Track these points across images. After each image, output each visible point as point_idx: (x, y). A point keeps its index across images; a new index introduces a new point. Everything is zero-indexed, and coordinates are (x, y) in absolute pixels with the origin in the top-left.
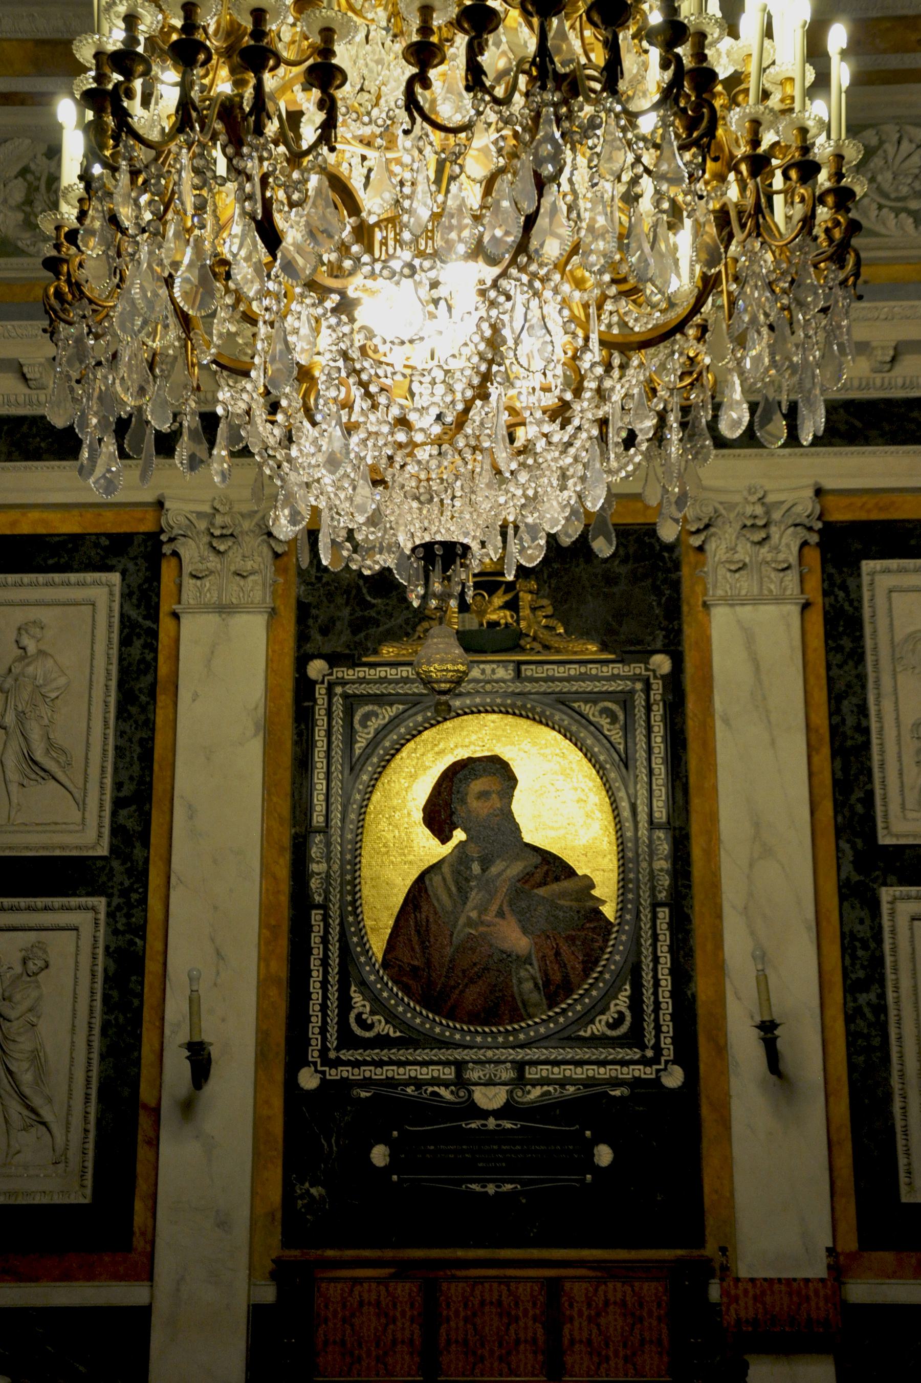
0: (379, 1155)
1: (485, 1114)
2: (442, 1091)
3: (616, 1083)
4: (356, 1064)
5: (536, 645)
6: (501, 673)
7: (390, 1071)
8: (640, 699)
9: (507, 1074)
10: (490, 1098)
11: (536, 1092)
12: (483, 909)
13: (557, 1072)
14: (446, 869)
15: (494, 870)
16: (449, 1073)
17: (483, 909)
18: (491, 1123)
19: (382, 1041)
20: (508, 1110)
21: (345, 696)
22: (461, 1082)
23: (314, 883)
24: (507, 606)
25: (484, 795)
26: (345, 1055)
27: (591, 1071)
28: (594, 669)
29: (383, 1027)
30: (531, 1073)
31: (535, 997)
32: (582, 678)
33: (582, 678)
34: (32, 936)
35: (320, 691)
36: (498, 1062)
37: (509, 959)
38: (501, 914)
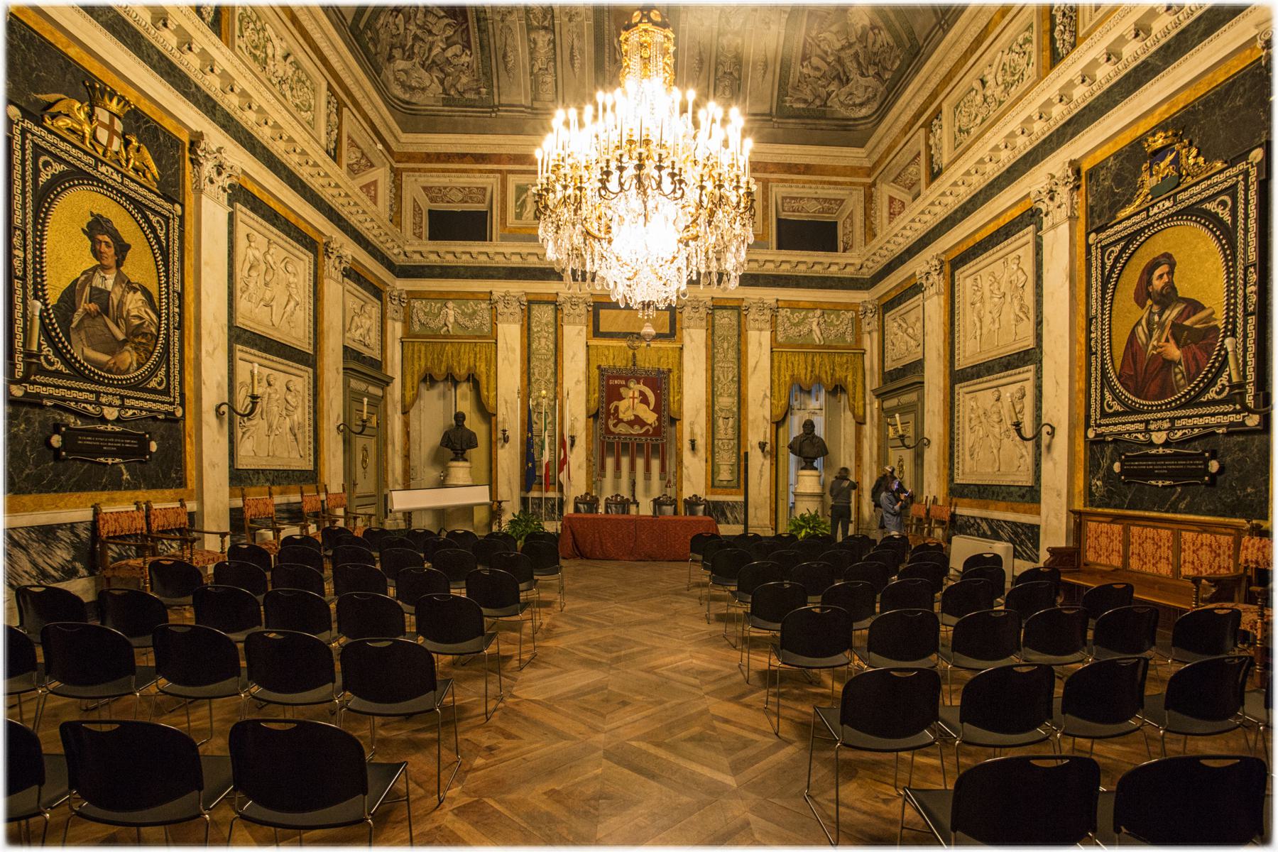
0: (1117, 467)
1: (1158, 446)
2: (1139, 436)
3: (1219, 426)
4: (1107, 425)
5: (1189, 179)
6: (1167, 204)
7: (1120, 428)
8: (1241, 186)
9: (1166, 425)
10: (1158, 438)
11: (1180, 433)
12: (1159, 340)
13: (1190, 422)
14: (1144, 322)
15: (1164, 317)
16: (1142, 427)
17: (1159, 340)
18: (1161, 450)
19: (1117, 414)
20: (1167, 444)
21: (1102, 248)
22: (1147, 431)
23: (1093, 343)
24: (1172, 162)
25: (1161, 276)
26: (1103, 422)
27: (1207, 420)
28: (1214, 180)
29: (1117, 407)
30: (1178, 423)
31: (1182, 382)
32: (1207, 189)
33: (1207, 189)
34: (1019, 385)
35: (1093, 248)
36: (1163, 419)
37: (1169, 364)
38: (1167, 340)
